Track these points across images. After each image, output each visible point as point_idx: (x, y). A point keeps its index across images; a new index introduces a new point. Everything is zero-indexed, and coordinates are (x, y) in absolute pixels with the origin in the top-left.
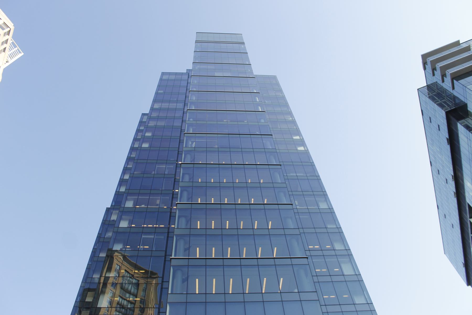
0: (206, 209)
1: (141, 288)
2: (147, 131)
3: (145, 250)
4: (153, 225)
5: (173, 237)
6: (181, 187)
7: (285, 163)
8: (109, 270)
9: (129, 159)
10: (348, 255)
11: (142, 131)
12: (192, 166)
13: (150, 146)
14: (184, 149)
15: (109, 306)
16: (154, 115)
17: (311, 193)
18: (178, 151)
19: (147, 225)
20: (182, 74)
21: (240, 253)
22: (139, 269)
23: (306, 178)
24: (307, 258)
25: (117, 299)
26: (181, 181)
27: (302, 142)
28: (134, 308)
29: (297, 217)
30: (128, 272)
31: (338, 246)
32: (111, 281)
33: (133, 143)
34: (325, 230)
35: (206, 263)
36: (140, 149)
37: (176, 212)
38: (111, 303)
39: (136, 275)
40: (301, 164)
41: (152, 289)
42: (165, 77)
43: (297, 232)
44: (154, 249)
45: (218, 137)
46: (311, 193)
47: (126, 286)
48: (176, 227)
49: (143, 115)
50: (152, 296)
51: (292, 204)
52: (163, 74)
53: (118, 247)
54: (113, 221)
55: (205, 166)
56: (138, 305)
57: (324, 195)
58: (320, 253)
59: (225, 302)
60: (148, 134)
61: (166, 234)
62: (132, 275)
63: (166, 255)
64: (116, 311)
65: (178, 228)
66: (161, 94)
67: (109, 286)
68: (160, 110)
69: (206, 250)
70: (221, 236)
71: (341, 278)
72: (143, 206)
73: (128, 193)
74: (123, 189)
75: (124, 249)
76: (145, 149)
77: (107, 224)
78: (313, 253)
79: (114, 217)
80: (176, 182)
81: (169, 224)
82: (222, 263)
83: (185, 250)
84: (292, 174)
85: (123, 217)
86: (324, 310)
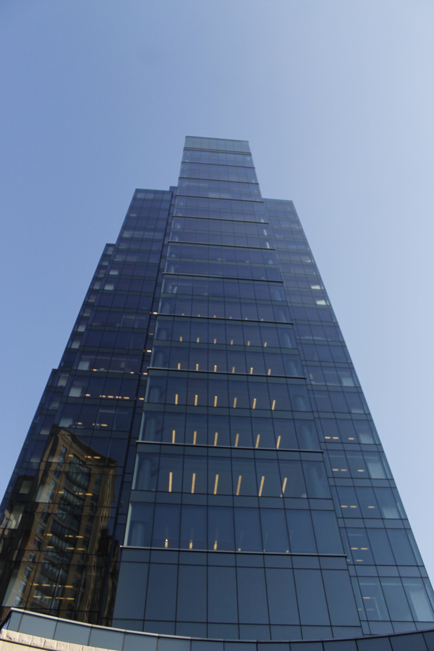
0: (188, 380)
3: (102, 428)
4: (115, 396)
5: (141, 414)
6: (156, 347)
8: (53, 453)
9: (86, 305)
10: (378, 452)
12: (171, 318)
13: (116, 290)
14: (162, 295)
15: (51, 501)
16: (123, 246)
17: (333, 365)
18: (154, 298)
19: (107, 396)
20: (163, 192)
21: (232, 441)
24: (322, 453)
25: (62, 492)
27: (323, 295)
28: (83, 505)
29: (311, 396)
31: (365, 439)
33: (93, 284)
34: (348, 416)
36: (101, 293)
37: (146, 381)
38: (52, 497)
39: (88, 463)
41: (109, 481)
42: (140, 196)
43: (310, 416)
44: (114, 429)
46: (333, 365)
47: (74, 476)
48: (146, 401)
50: (108, 491)
51: (305, 379)
52: (138, 191)
53: (66, 423)
54: (61, 387)
55: (189, 319)
56: (88, 502)
57: (349, 368)
58: (340, 447)
59: (207, 506)
60: (114, 273)
62: (82, 461)
63: (130, 438)
64: (59, 508)
65: (148, 402)
67: (51, 475)
68: (131, 240)
69: (184, 435)
70: (206, 417)
71: (367, 483)
72: (102, 369)
74: (76, 345)
75: (74, 427)
76: (109, 293)
77: (52, 391)
78: (330, 446)
79: (62, 383)
80: (148, 341)
84: (307, 338)
86: (342, 525)
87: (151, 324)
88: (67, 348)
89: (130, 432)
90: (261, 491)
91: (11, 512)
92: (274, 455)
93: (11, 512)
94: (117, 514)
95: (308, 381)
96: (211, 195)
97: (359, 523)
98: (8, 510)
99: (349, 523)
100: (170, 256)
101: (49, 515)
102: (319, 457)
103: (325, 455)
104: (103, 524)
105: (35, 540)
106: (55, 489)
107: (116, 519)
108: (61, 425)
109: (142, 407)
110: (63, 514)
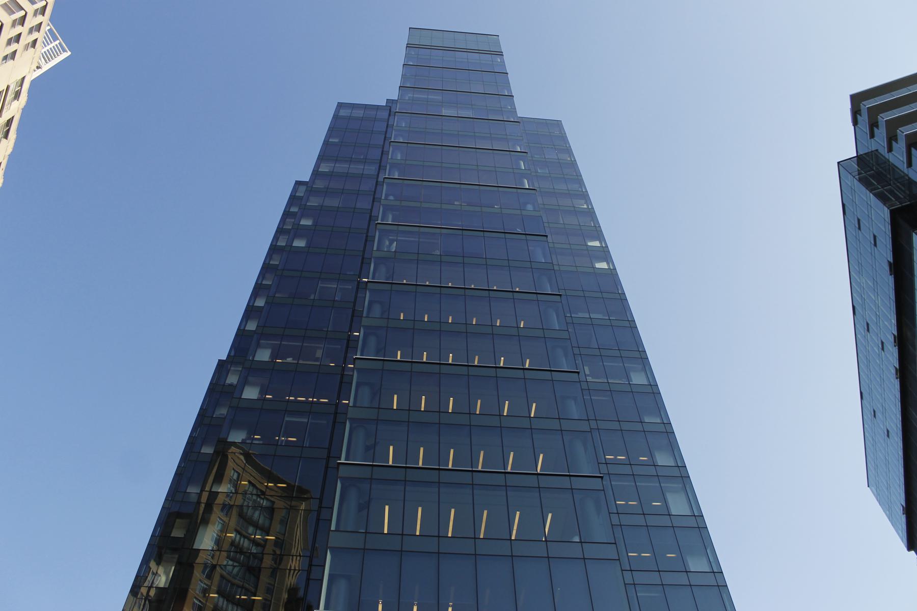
1: (278, 516)
2: (303, 216)
4: (307, 399)
5: (345, 423)
6: (366, 327)
7: (569, 293)
8: (219, 479)
9: (266, 268)
10: (680, 476)
11: (294, 215)
12: (388, 287)
13: (309, 246)
14: (375, 254)
16: (320, 184)
17: (617, 353)
18: (363, 258)
20: (377, 108)
21: (473, 461)
22: (277, 480)
23: (608, 323)
24: (602, 477)
26: (365, 315)
27: (604, 253)
30: (254, 485)
31: (663, 459)
32: (220, 499)
33: (276, 238)
34: (638, 427)
35: (404, 479)
36: (288, 250)
38: (218, 542)
39: (268, 492)
40: (599, 295)
41: (299, 520)
42: (343, 113)
43: (585, 426)
44: (306, 444)
45: (441, 234)
46: (617, 353)
47: (250, 512)
48: (351, 404)
49: (298, 183)
50: (298, 533)
51: (578, 373)
52: (340, 105)
53: (237, 436)
54: (231, 385)
55: (413, 288)
58: (627, 470)
61: (332, 416)
62: (261, 491)
63: (329, 457)
64: (228, 557)
65: (354, 406)
66: (334, 144)
67: (216, 511)
68: (331, 175)
71: (666, 521)
72: (289, 360)
73: (261, 335)
74: (252, 326)
75: (248, 441)
77: (218, 391)
78: (613, 469)
79: (232, 379)
80: (355, 317)
81: (339, 398)
82: (436, 480)
83: (367, 448)
84: (580, 315)
85: (250, 379)
86: (629, 580)
87: (359, 295)
88: (239, 329)
89: (329, 450)
90: (514, 532)
91: (158, 564)
92: (532, 481)
93: (158, 564)
94: (310, 565)
95: (582, 378)
96: (444, 112)
97: (654, 578)
98: (155, 560)
99: (640, 578)
100: (386, 199)
101: (214, 567)
102: (596, 484)
103: (606, 482)
104: (291, 581)
105: (194, 603)
106: (221, 531)
107: (309, 572)
108: (231, 439)
109: (346, 414)
110: (235, 566)
